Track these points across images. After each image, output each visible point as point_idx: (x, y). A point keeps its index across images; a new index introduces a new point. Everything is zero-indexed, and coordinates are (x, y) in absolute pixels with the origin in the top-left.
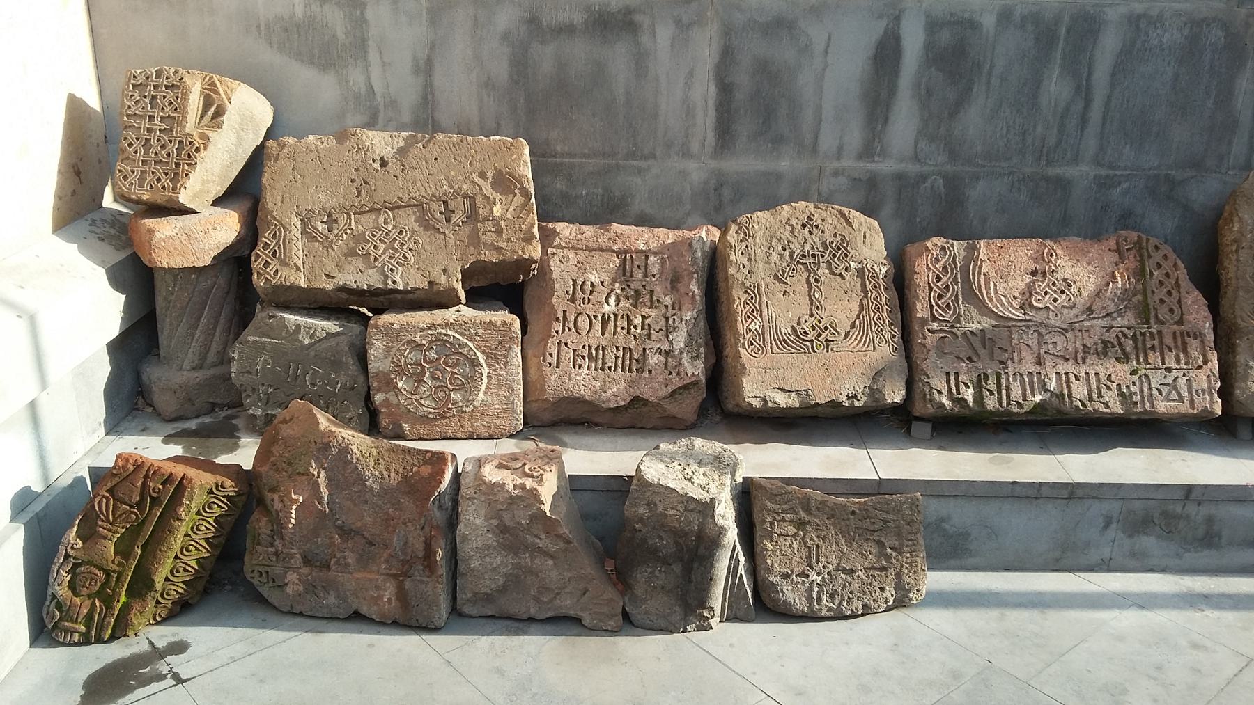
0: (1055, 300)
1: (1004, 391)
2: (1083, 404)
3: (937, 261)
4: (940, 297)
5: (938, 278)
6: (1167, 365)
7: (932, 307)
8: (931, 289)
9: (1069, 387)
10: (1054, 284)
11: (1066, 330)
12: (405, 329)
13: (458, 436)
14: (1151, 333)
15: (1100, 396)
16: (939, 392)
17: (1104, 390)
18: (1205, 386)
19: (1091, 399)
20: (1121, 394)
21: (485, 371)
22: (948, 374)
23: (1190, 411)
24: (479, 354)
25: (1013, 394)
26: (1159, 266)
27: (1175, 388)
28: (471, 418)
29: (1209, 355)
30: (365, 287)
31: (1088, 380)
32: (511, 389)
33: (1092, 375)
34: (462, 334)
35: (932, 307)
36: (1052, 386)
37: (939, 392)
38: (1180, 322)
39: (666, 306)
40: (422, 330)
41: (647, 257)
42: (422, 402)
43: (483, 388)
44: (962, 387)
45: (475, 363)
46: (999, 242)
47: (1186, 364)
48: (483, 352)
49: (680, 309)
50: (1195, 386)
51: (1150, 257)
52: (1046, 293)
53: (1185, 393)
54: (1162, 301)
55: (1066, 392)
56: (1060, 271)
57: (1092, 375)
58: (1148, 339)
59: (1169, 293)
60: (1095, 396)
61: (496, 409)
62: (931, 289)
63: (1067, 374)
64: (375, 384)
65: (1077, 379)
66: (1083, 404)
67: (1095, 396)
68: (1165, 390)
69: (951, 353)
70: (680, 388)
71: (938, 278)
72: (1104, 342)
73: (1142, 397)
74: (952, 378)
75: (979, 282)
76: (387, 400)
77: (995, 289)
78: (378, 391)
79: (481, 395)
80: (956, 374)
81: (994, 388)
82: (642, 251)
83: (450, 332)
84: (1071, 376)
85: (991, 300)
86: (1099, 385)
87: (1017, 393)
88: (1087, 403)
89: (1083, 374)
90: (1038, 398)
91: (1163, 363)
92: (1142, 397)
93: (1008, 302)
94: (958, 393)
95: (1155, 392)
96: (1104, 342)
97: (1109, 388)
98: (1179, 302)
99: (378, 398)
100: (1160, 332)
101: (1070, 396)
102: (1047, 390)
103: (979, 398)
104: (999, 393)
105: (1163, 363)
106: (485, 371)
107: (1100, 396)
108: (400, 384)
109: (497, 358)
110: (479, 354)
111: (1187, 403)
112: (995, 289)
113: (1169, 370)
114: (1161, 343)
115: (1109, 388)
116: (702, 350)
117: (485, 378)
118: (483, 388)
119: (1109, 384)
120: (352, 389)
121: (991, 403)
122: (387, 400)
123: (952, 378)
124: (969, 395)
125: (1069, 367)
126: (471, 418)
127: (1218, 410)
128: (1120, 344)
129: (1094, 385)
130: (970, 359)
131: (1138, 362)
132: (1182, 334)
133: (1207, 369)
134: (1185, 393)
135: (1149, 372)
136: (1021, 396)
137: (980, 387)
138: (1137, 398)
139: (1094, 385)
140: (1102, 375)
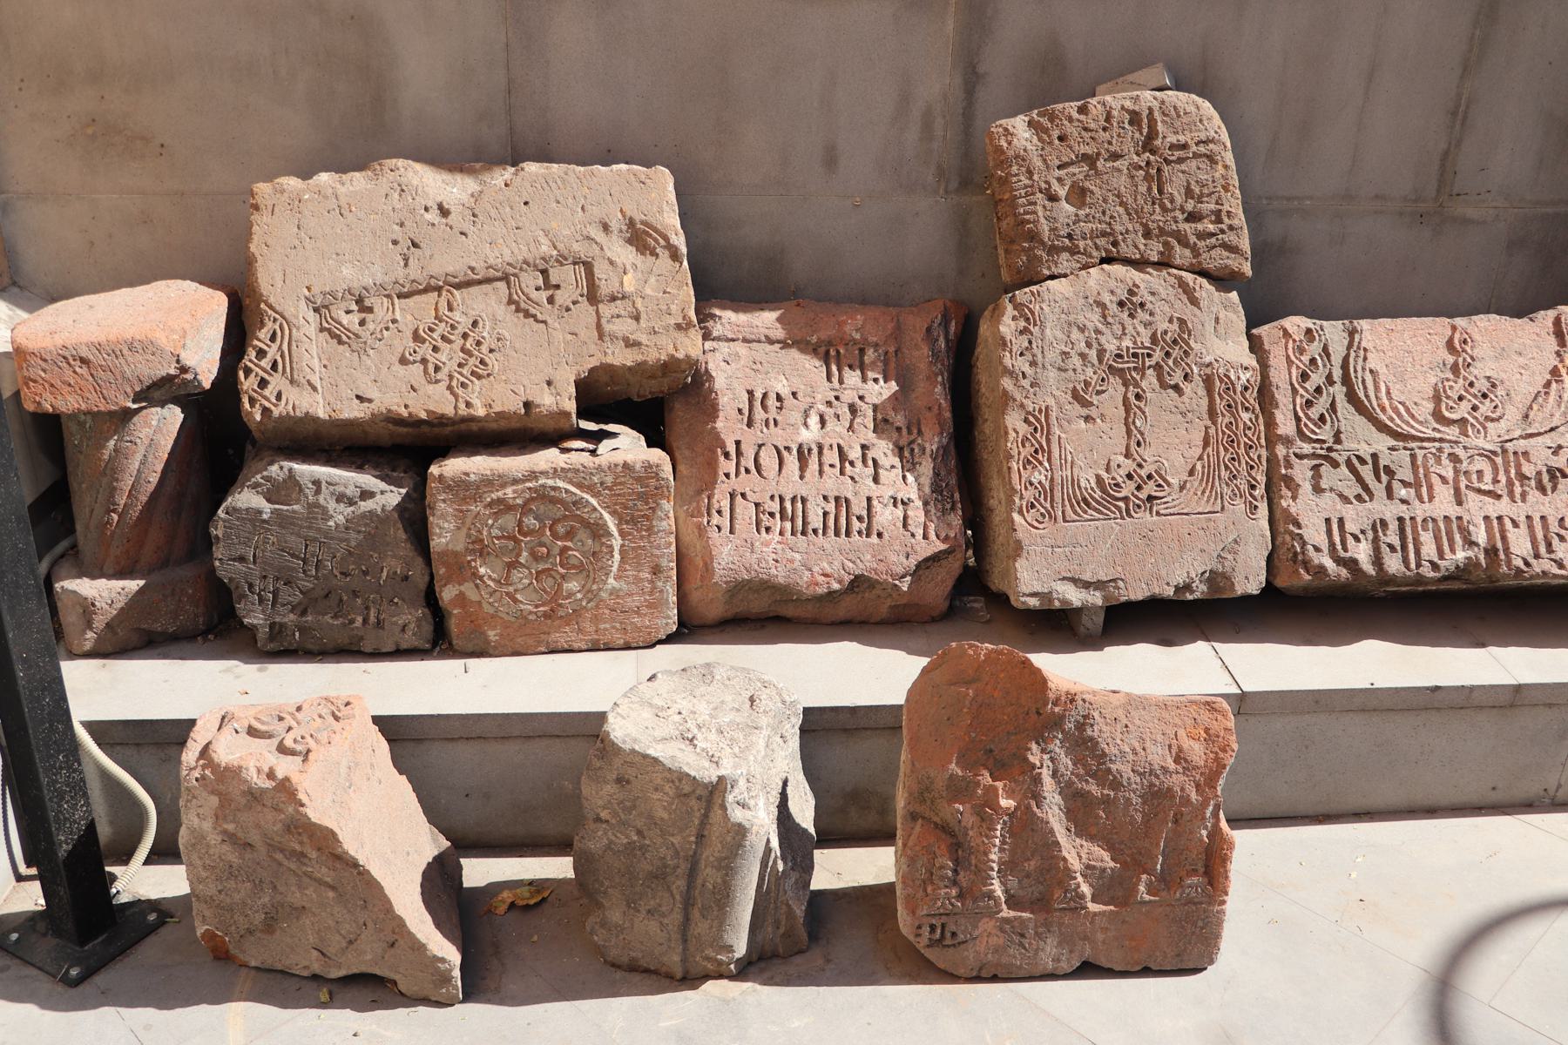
0: (1475, 408)
1: (1411, 547)
2: (1527, 564)
3: (1301, 351)
4: (1309, 404)
5: (1304, 377)
7: (1298, 419)
9: (1504, 538)
10: (1471, 384)
12: (489, 482)
13: (576, 646)
17: (1555, 541)
19: (1537, 556)
21: (617, 542)
24: (607, 516)
28: (596, 619)
30: (423, 415)
31: (1531, 527)
32: (656, 570)
34: (579, 486)
35: (1298, 419)
36: (1481, 537)
37: (1317, 549)
39: (899, 429)
40: (515, 481)
41: (862, 351)
42: (518, 596)
43: (615, 569)
44: (1350, 541)
45: (598, 531)
46: (1387, 322)
48: (613, 513)
49: (920, 432)
52: (1461, 398)
55: (1499, 545)
60: (1543, 550)
61: (635, 601)
63: (1499, 518)
64: (442, 571)
65: (1515, 524)
66: (1527, 564)
67: (1543, 550)
69: (1331, 490)
70: (927, 560)
71: (1304, 377)
72: (1550, 471)
75: (1364, 381)
76: (461, 595)
77: (1388, 393)
78: (448, 581)
79: (611, 581)
80: (1341, 521)
81: (1397, 542)
82: (855, 342)
83: (561, 484)
85: (1383, 409)
87: (1429, 550)
89: (1522, 519)
90: (1461, 555)
94: (1345, 550)
96: (1550, 471)
99: (447, 594)
101: (1507, 550)
102: (1471, 543)
103: (1377, 560)
106: (617, 542)
108: (482, 570)
109: (636, 518)
110: (607, 516)
112: (1388, 393)
116: (957, 496)
117: (617, 557)
118: (615, 569)
120: (406, 578)
122: (461, 595)
124: (1362, 552)
125: (1503, 507)
126: (596, 619)
129: (1540, 535)
130: (1359, 498)
136: (1438, 557)
139: (1540, 535)
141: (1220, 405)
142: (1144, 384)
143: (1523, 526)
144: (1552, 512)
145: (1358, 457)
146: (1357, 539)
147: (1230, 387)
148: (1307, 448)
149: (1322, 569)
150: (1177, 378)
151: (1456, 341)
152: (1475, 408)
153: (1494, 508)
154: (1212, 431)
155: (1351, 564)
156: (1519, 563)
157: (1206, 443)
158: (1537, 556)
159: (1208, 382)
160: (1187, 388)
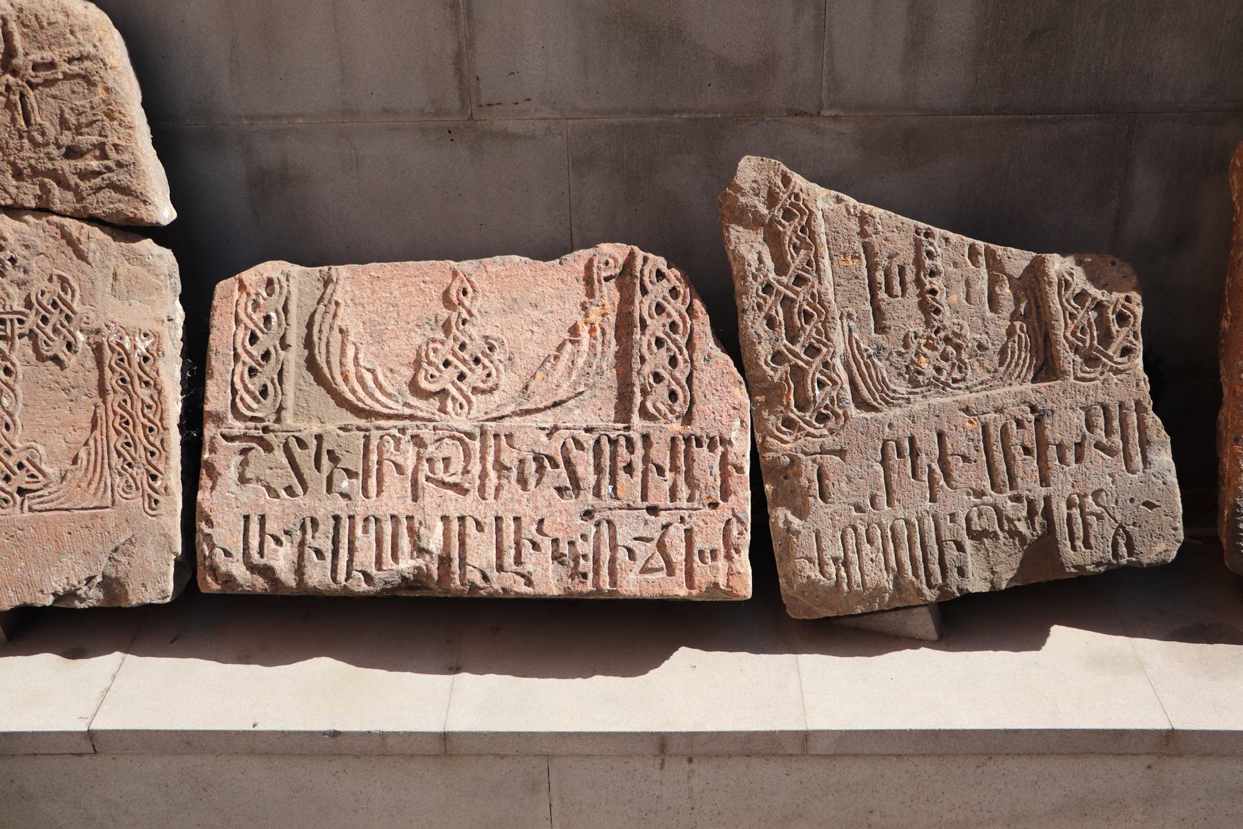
2: (485, 578)
6: (652, 501)
7: (234, 391)
8: (236, 357)
10: (463, 346)
11: (471, 436)
14: (629, 440)
15: (518, 561)
16: (227, 554)
18: (719, 544)
19: (500, 568)
20: (557, 557)
22: (247, 518)
23: (682, 592)
25: (358, 557)
26: (660, 309)
27: (661, 546)
29: (734, 481)
31: (499, 530)
33: (509, 527)
35: (234, 391)
36: (434, 542)
37: (227, 554)
38: (688, 418)
44: (270, 544)
47: (690, 499)
50: (699, 543)
51: (644, 291)
52: (447, 364)
53: (678, 557)
54: (658, 377)
55: (455, 554)
56: (479, 320)
57: (509, 527)
58: (622, 450)
59: (673, 361)
60: (509, 560)
62: (236, 357)
65: (479, 526)
66: (485, 578)
67: (509, 560)
68: (641, 549)
69: (258, 480)
71: (253, 339)
73: (596, 561)
74: (254, 527)
77: (356, 358)
80: (263, 519)
81: (327, 547)
84: (470, 524)
85: (346, 379)
86: (522, 541)
87: (366, 558)
88: (493, 574)
89: (489, 521)
90: (407, 564)
91: (644, 497)
92: (596, 561)
93: (376, 380)
94: (261, 554)
95: (622, 554)
97: (536, 546)
98: (689, 380)
100: (646, 438)
101: (463, 564)
102: (420, 551)
103: (299, 570)
104: (335, 553)
105: (644, 497)
107: (518, 561)
111: (680, 575)
112: (356, 358)
113: (653, 510)
114: (646, 459)
115: (536, 546)
119: (538, 538)
121: (318, 576)
123: (254, 527)
124: (281, 560)
125: (468, 504)
127: (745, 588)
128: (568, 463)
130: (290, 490)
131: (597, 493)
132: (687, 440)
133: (725, 511)
134: (678, 557)
135: (616, 516)
136: (373, 565)
137: (302, 544)
138: (586, 566)
140: (525, 521)
141: (111, 380)
142: (14, 357)
143: (490, 528)
144: (529, 511)
145: (298, 440)
146: (278, 541)
147: (124, 358)
148: (238, 427)
149: (229, 579)
150: (58, 348)
151: (453, 293)
152: (462, 377)
153: (455, 505)
154: (101, 411)
155: (267, 572)
156: (477, 578)
157: (94, 426)
158: (500, 568)
159: (98, 350)
160: (71, 360)
